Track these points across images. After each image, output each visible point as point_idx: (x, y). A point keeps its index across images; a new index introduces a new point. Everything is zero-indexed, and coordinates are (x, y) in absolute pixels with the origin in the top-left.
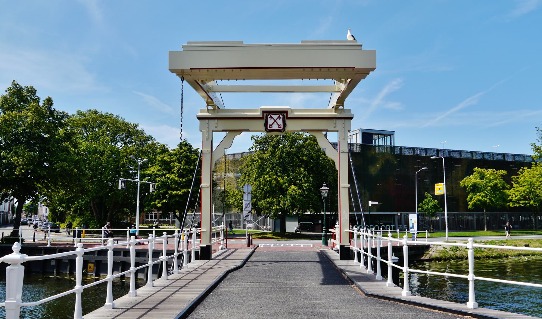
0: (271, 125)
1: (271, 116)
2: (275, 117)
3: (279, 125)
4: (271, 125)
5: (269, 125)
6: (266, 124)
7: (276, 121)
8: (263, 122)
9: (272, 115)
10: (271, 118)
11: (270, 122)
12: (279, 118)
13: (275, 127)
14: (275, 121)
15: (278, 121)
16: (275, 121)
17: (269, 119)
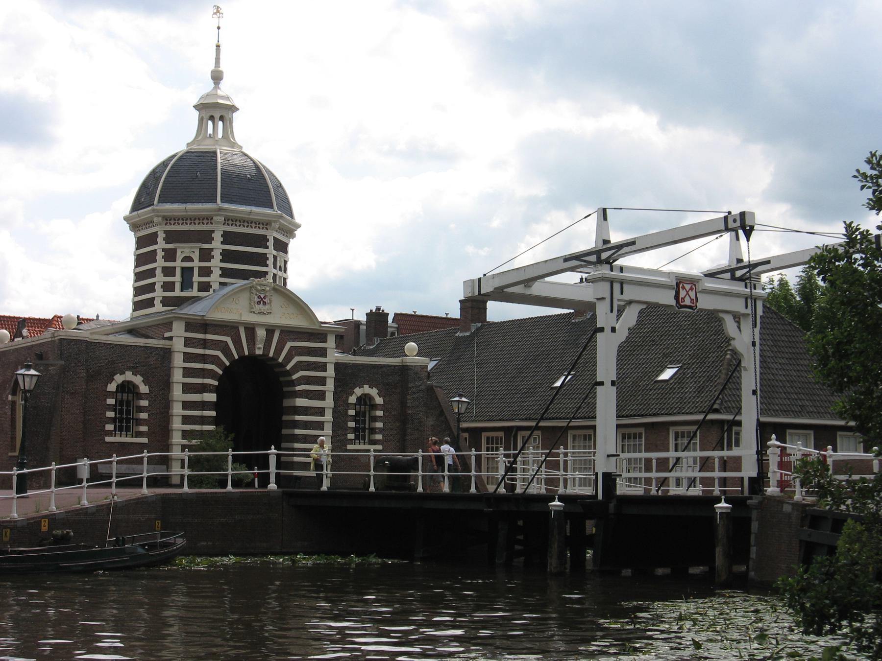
0: (683, 299)
1: (683, 285)
2: (688, 287)
3: (692, 300)
4: (683, 299)
5: (682, 298)
6: (677, 297)
7: (689, 293)
8: (673, 293)
9: (684, 284)
10: (684, 288)
11: (682, 293)
12: (691, 289)
13: (687, 302)
14: (687, 292)
15: (690, 293)
16: (687, 292)
17: (681, 289)
